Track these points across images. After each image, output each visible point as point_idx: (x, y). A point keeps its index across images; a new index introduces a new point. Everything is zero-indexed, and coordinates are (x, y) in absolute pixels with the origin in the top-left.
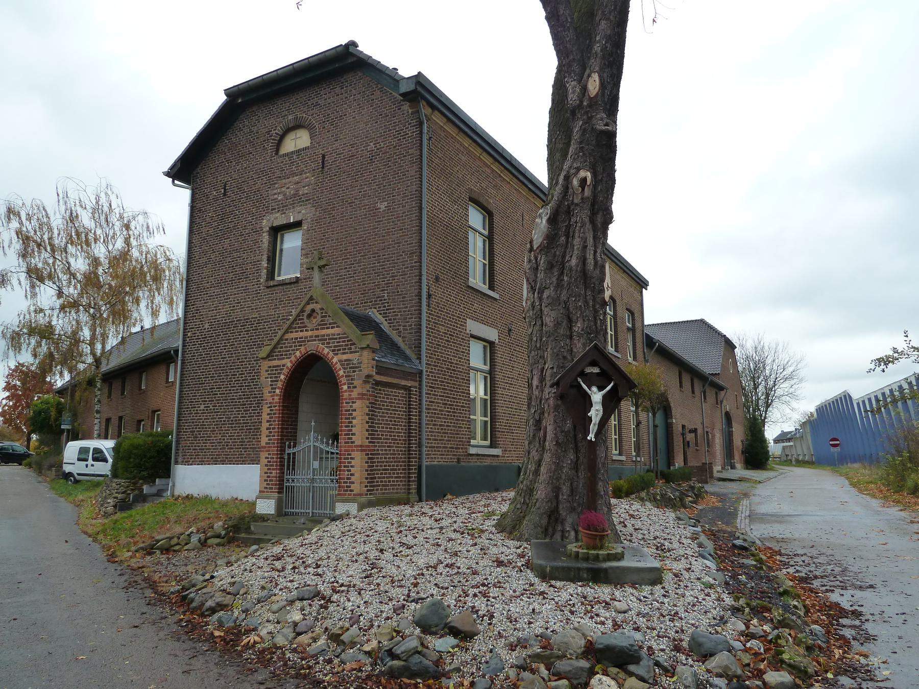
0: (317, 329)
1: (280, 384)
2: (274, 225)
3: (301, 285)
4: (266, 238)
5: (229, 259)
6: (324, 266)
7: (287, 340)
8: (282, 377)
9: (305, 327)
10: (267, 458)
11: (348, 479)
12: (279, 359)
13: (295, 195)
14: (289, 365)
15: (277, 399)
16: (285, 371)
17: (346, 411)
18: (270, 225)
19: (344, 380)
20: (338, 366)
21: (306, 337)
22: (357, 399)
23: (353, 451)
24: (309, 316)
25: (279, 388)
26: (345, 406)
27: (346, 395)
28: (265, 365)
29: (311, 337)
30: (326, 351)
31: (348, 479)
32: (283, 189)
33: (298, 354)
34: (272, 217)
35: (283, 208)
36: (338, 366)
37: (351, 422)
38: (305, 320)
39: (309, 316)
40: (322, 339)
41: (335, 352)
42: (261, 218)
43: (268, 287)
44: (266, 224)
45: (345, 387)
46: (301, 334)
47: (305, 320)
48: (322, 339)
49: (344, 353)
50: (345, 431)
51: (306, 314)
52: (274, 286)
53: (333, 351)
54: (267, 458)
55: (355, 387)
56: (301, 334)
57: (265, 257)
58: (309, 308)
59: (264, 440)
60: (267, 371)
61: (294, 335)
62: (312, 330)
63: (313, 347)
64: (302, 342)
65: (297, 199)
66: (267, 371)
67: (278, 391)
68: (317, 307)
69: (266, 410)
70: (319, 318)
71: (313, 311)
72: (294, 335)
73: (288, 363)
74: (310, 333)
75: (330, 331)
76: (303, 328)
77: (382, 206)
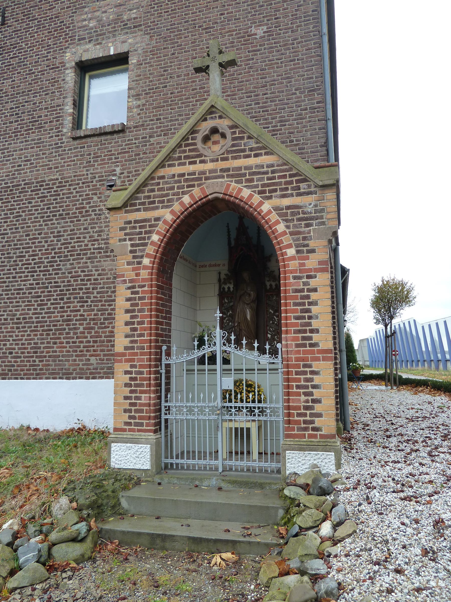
0: (223, 159)
1: (150, 249)
2: (83, 59)
3: (129, 135)
4: (70, 76)
5: (12, 105)
6: (232, 63)
7: (163, 177)
8: (155, 238)
9: (200, 156)
10: (126, 372)
11: (306, 408)
12: (145, 210)
13: (115, 21)
14: (169, 217)
15: (144, 274)
16: (161, 227)
17: (297, 291)
18: (77, 59)
19: (286, 240)
20: (274, 217)
21: (203, 173)
22: (316, 270)
23: (318, 359)
24: (206, 139)
25: (148, 256)
26: (290, 284)
27: (293, 265)
28: (118, 220)
29: (211, 171)
30: (246, 193)
31: (306, 408)
32: (98, 14)
33: (187, 199)
34: (80, 49)
35: (96, 37)
36: (274, 217)
37: (309, 311)
38: (200, 145)
39: (206, 139)
40: (237, 175)
41: (266, 193)
42: (63, 50)
43: (75, 139)
44: (71, 57)
45: (291, 252)
46: (192, 168)
47: (200, 145)
48: (237, 175)
49: (284, 196)
50: (296, 325)
51: (199, 136)
52: (86, 137)
53: (260, 193)
54: (126, 372)
55: (313, 251)
56: (192, 168)
57: (69, 101)
58: (205, 127)
59: (121, 343)
60: (122, 229)
61: (177, 170)
62: (212, 161)
63: (215, 188)
65: (121, 25)
66: (122, 229)
67: (146, 261)
68: (223, 124)
70: (229, 142)
71: (214, 131)
72: (177, 170)
73: (168, 216)
74: (210, 166)
75: (252, 161)
76: (197, 157)
77: (260, 32)
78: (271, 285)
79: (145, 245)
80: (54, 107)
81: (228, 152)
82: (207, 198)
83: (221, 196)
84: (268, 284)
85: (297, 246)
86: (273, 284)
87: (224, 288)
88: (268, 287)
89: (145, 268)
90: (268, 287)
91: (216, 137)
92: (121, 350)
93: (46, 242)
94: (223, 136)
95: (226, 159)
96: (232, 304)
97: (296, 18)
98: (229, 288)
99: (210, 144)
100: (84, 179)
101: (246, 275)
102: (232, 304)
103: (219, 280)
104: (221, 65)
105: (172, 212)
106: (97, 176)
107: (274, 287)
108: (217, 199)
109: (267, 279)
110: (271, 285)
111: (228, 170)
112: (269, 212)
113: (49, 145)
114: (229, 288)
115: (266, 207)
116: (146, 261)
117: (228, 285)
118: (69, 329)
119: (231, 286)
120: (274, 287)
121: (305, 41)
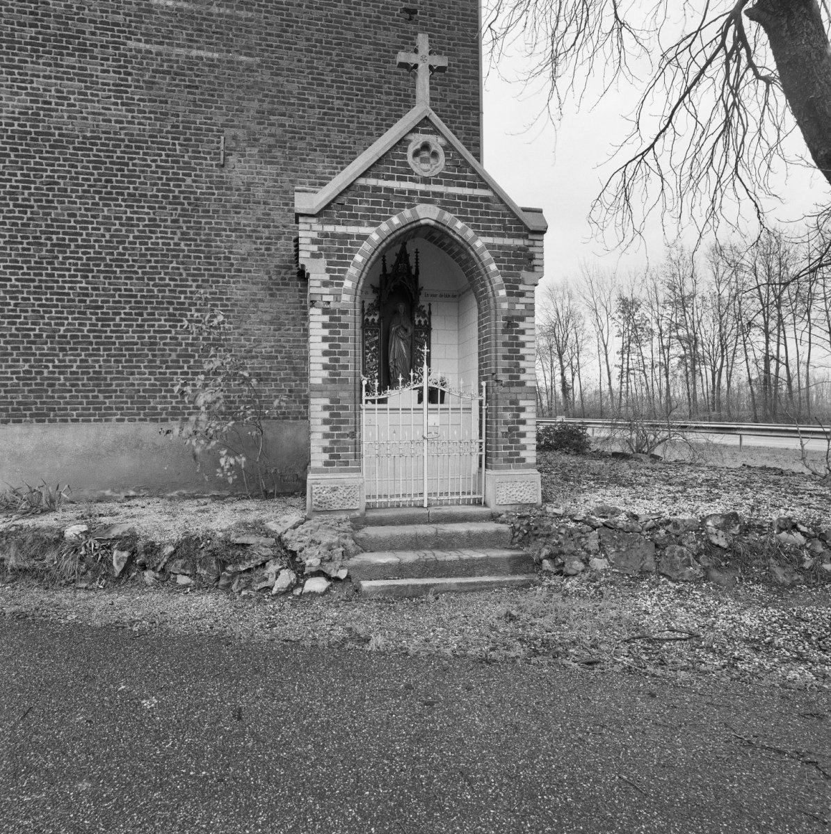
14: (375, 237)
20: (487, 255)
33: (395, 220)
36: (487, 255)
38: (410, 160)
39: (416, 154)
53: (473, 227)
58: (417, 140)
63: (428, 213)
64: (409, 199)
66: (314, 242)
68: (436, 143)
69: (317, 318)
71: (426, 147)
73: (375, 235)
76: (406, 173)
78: (420, 321)
79: (348, 264)
80: (107, 23)
81: (442, 175)
82: (418, 223)
83: (433, 223)
84: (417, 320)
85: (507, 287)
86: (423, 321)
87: (367, 320)
89: (346, 292)
91: (426, 154)
92: (319, 381)
93: (109, 230)
94: (435, 155)
95: (439, 183)
96: (377, 338)
97: (454, 14)
98: (373, 320)
99: (418, 159)
100: (169, 150)
102: (377, 338)
103: (363, 310)
104: (431, 67)
105: (378, 232)
106: (190, 150)
108: (427, 225)
110: (420, 321)
111: (441, 195)
112: (482, 250)
113: (103, 84)
114: (373, 320)
115: (479, 243)
116: (348, 284)
117: (420, 318)
118: (154, 356)
119: (376, 318)
121: (463, 46)
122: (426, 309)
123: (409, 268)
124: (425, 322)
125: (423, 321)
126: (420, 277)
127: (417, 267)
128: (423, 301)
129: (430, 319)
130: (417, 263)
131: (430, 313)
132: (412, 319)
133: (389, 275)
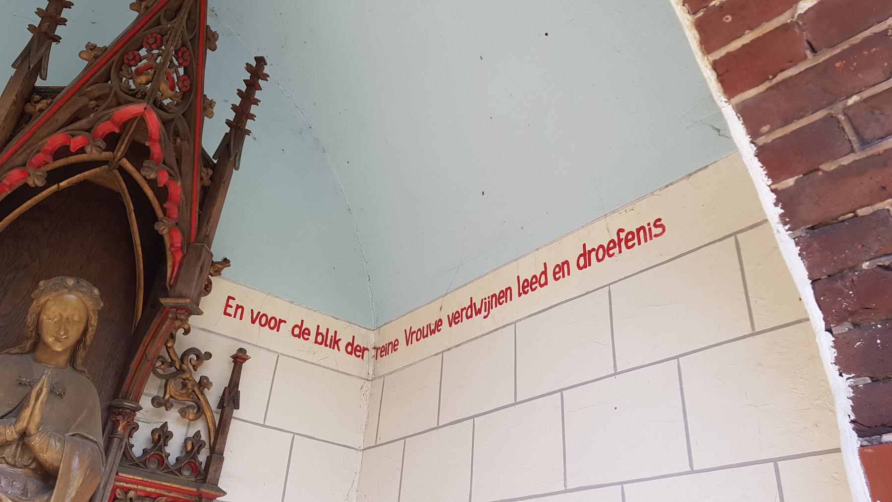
78: (162, 436)
84: (147, 420)
86: (180, 431)
88: (140, 441)
90: (140, 441)
101: (66, 309)
107: (173, 450)
109: (152, 387)
110: (162, 436)
120: (173, 450)
122: (217, 371)
123: (195, 105)
124: (193, 444)
125: (180, 431)
126: (239, 184)
127: (237, 130)
128: (210, 331)
129: (221, 430)
130: (248, 97)
131: (231, 398)
132: (117, 414)
133: (50, 93)
